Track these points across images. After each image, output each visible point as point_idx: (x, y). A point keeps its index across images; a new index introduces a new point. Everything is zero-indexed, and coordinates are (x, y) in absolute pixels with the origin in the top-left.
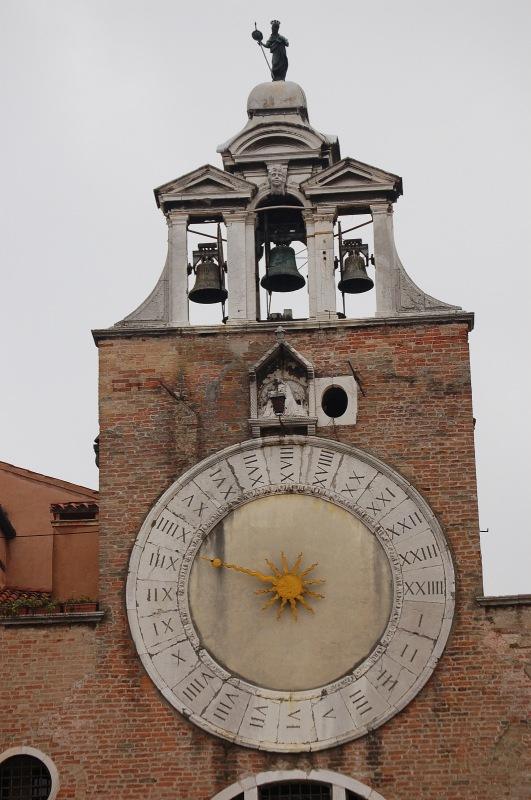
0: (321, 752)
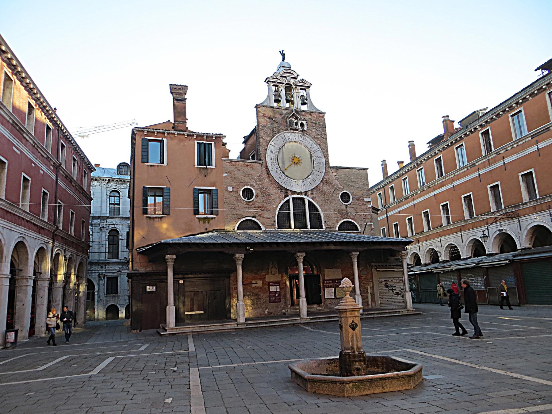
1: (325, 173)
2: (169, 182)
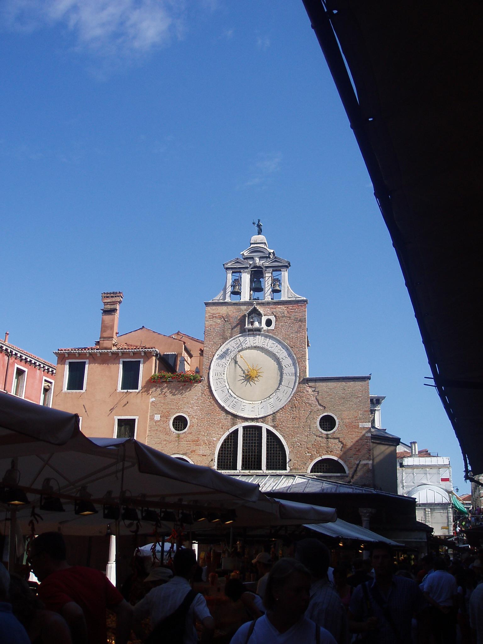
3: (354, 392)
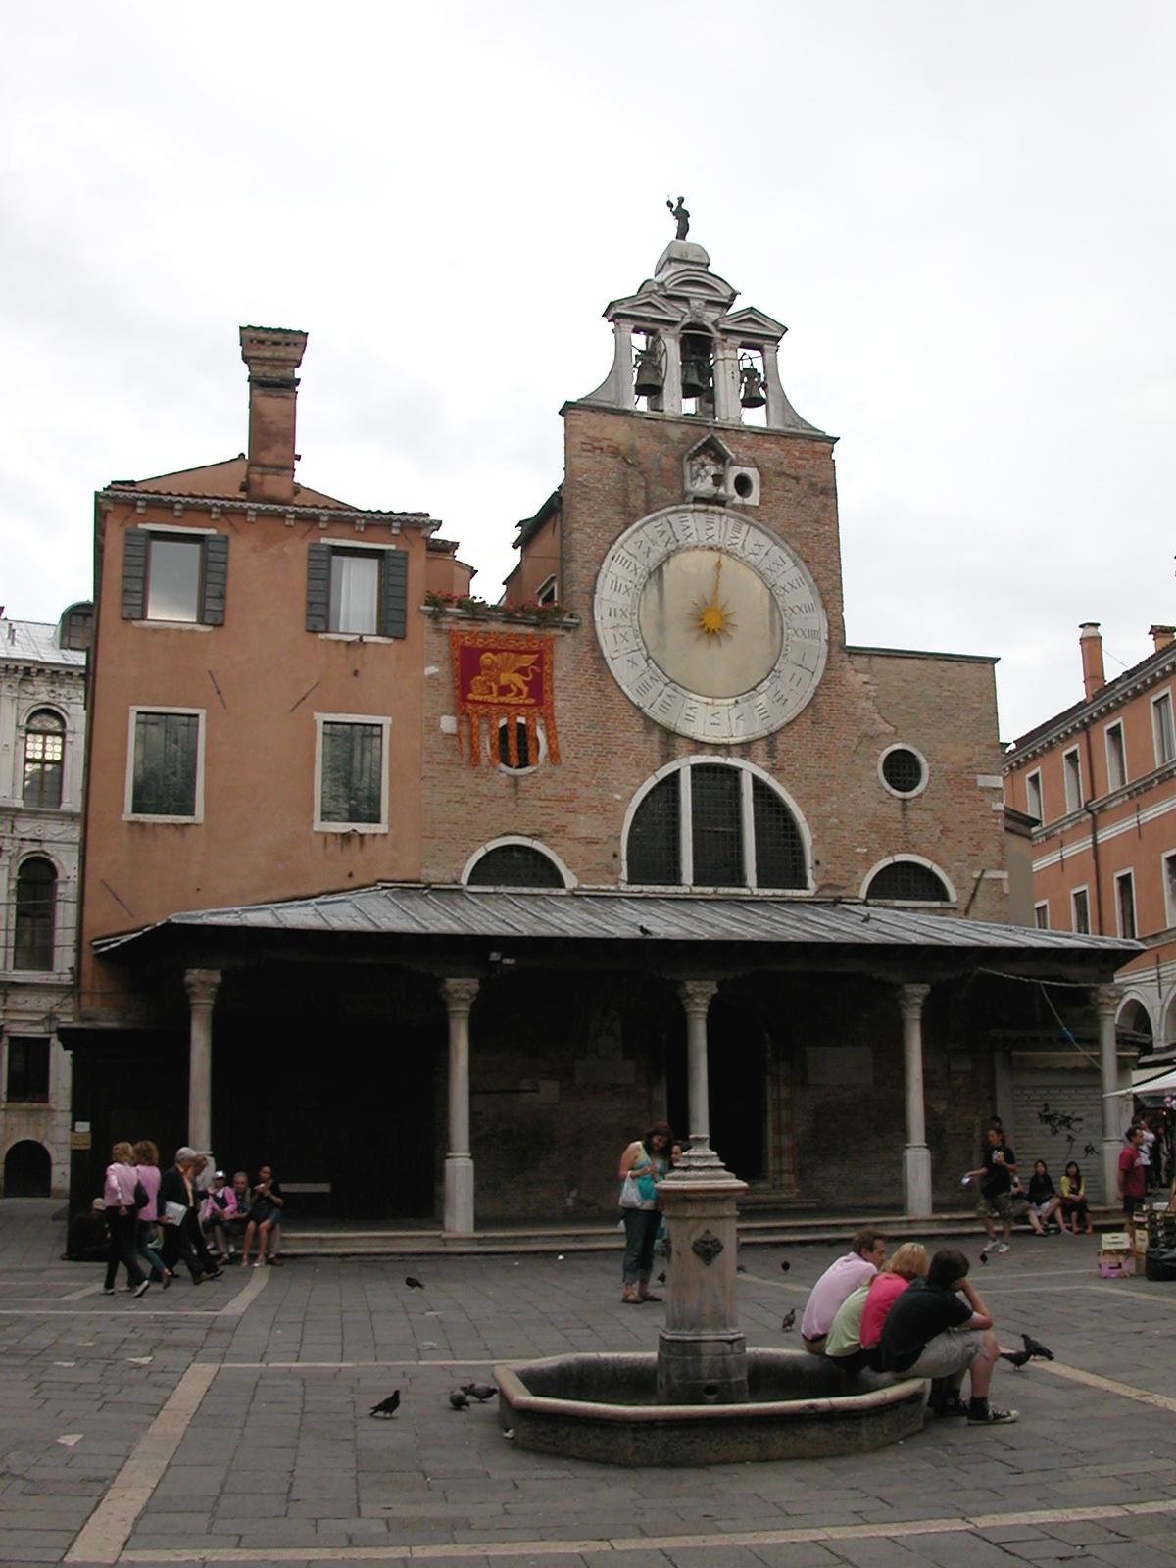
0: (736, 745)
1: (824, 673)
2: (219, 693)
3: (962, 695)
